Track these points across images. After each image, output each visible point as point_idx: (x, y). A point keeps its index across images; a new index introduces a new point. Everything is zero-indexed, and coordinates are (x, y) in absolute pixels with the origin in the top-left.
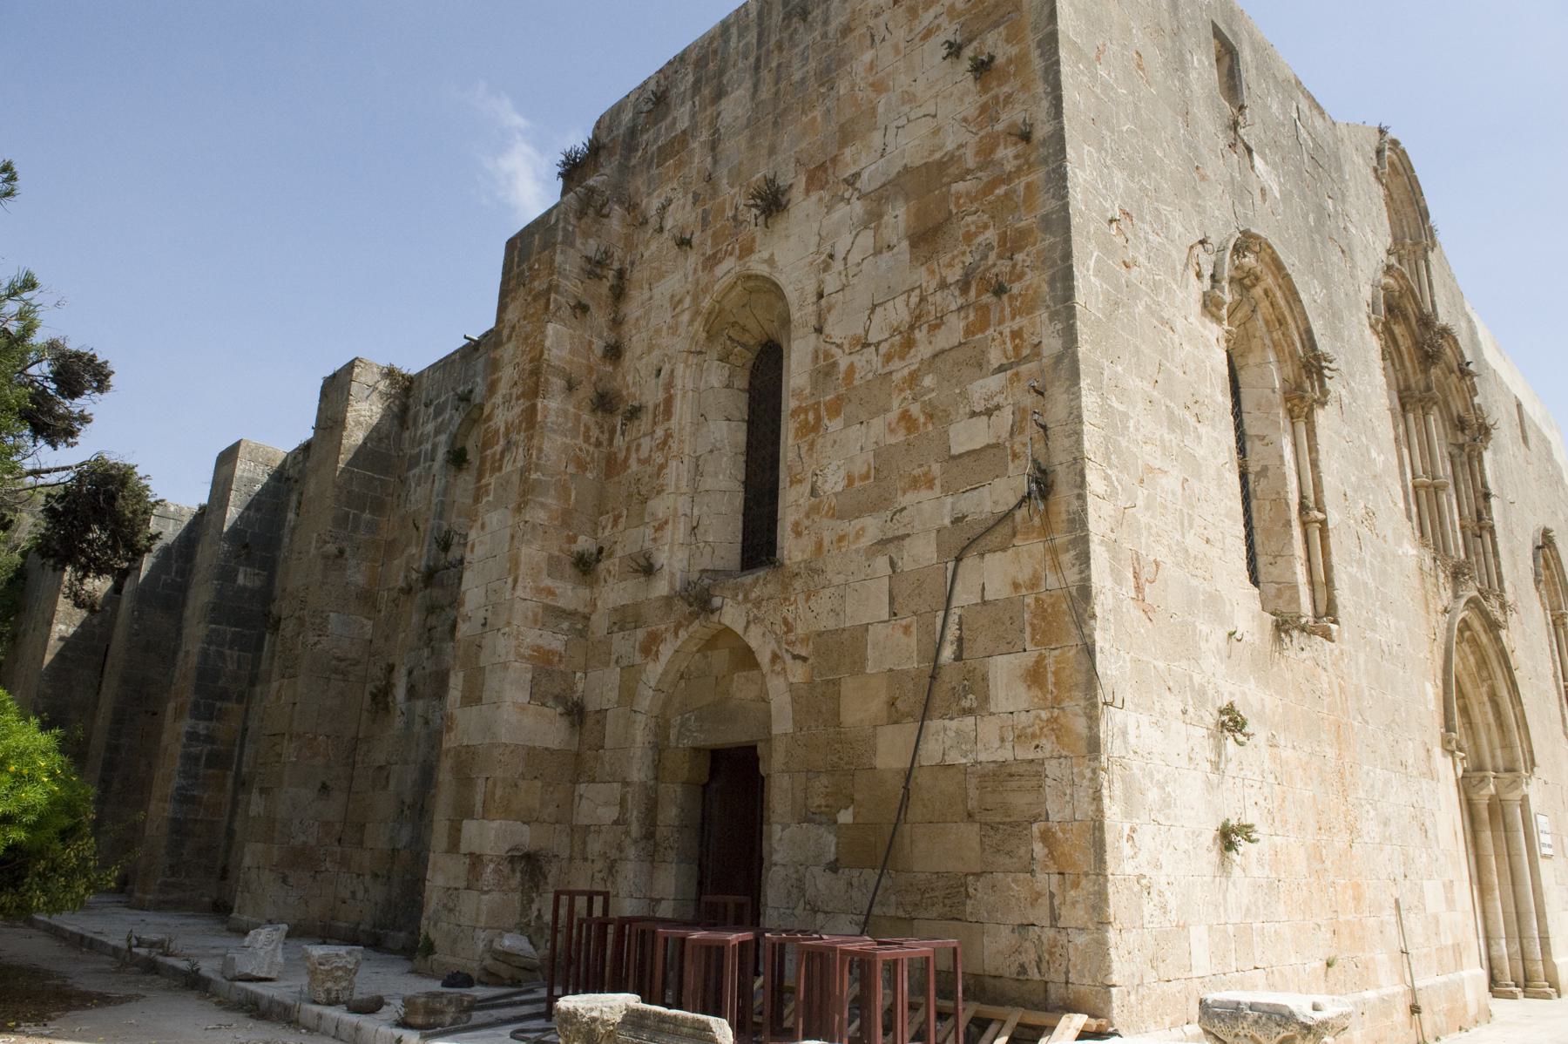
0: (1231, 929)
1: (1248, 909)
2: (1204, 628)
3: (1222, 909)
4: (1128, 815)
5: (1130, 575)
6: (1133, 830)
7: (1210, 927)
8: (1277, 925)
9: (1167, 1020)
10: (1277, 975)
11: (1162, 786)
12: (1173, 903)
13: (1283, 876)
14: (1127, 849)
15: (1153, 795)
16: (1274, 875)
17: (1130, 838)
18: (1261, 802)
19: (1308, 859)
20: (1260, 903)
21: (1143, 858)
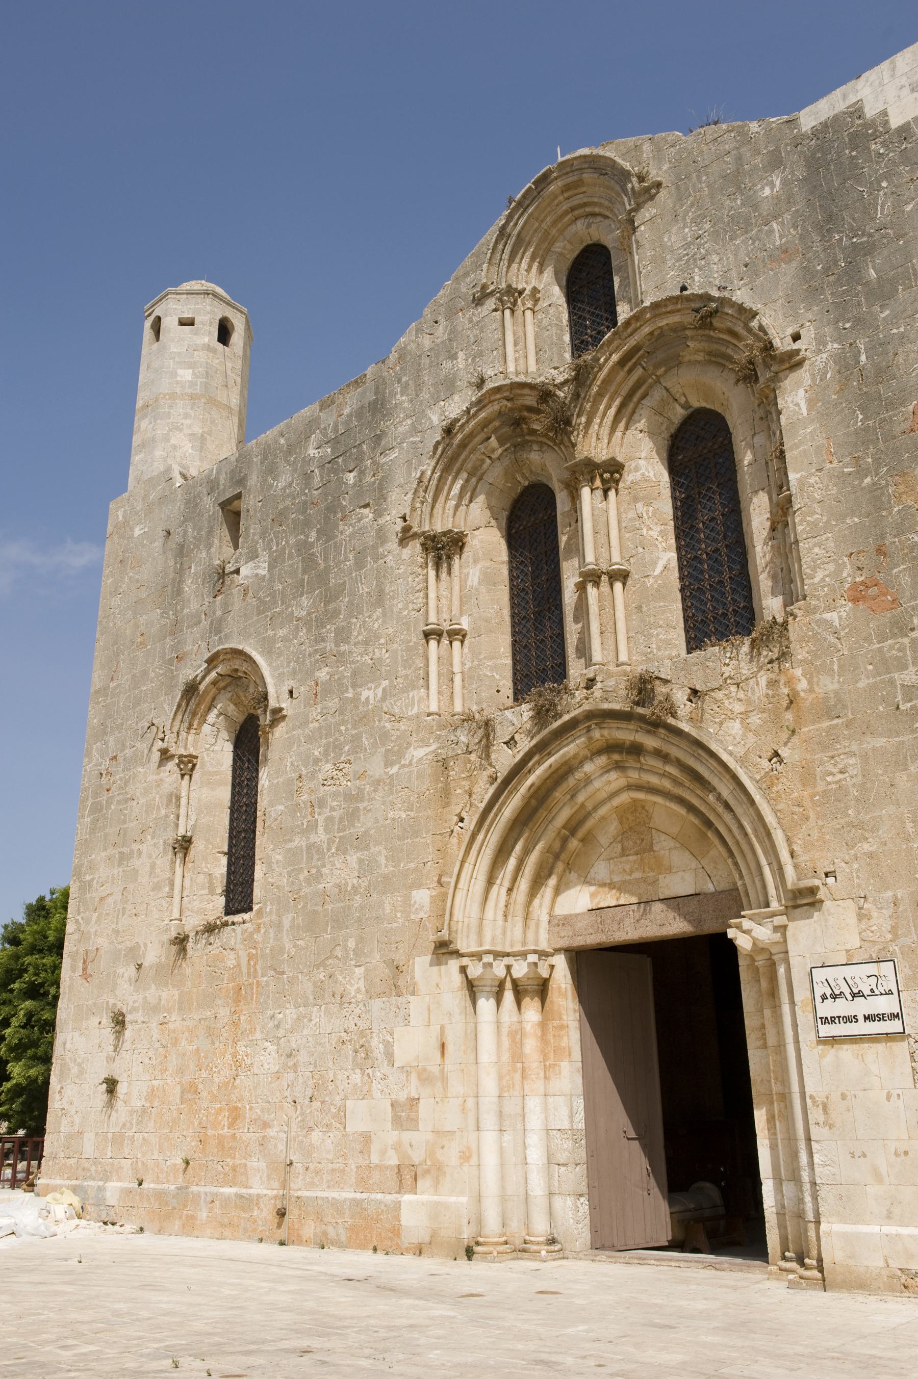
0: (110, 1135)
1: (124, 1125)
2: (120, 971)
3: (106, 1125)
4: (60, 1082)
5: (81, 965)
6: (62, 1088)
7: (97, 1134)
8: (146, 1135)
9: (66, 1176)
10: (140, 1164)
11: (79, 1065)
12: (77, 1120)
13: (156, 1104)
14: (57, 1097)
15: (75, 1070)
16: (148, 1104)
17: (60, 1092)
18: (146, 1061)
19: (182, 1093)
20: (134, 1122)
21: (65, 1100)
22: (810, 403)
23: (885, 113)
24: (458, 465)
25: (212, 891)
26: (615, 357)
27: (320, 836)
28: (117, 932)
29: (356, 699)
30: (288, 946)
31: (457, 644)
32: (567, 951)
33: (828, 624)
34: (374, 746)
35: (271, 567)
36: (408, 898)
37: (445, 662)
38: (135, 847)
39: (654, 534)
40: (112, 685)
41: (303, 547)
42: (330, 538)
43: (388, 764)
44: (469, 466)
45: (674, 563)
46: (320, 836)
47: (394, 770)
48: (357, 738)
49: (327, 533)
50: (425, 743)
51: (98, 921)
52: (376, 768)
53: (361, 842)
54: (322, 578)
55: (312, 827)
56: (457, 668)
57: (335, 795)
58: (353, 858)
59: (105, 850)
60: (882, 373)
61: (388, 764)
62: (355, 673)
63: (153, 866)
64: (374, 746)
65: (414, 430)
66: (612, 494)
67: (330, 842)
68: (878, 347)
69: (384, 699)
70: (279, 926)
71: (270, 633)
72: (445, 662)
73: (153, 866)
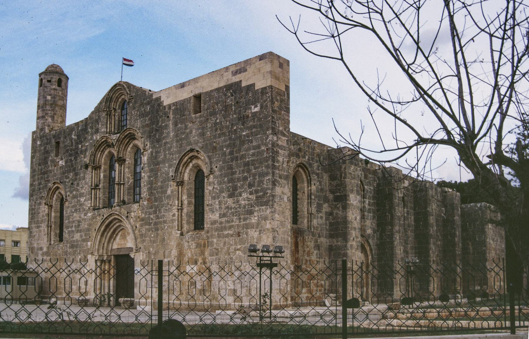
2: (39, 252)
22: (147, 160)
23: (163, 101)
24: (98, 150)
25: (56, 236)
26: (123, 137)
27: (74, 229)
28: (38, 244)
29: (80, 200)
30: (68, 251)
31: (98, 191)
32: (114, 255)
33: (144, 204)
34: (83, 211)
35: (65, 163)
36: (87, 243)
37: (96, 195)
38: (40, 225)
39: (129, 176)
40: (34, 183)
41: (71, 160)
42: (76, 160)
43: (85, 216)
44: (101, 150)
45: (133, 182)
46: (74, 229)
47: (86, 217)
48: (80, 209)
49: (76, 158)
50: (91, 213)
51: (34, 240)
52: (82, 216)
53: (80, 231)
54: (74, 170)
55: (72, 227)
56: (98, 196)
57: (76, 220)
58: (79, 234)
59: (34, 224)
60: (156, 158)
61: (85, 216)
62: (80, 194)
63: (44, 230)
64: (83, 211)
65: (91, 139)
66: (123, 166)
67: (75, 230)
68: (156, 152)
69: (85, 201)
70: (67, 246)
71: (65, 180)
72: (96, 195)
73: (44, 230)
